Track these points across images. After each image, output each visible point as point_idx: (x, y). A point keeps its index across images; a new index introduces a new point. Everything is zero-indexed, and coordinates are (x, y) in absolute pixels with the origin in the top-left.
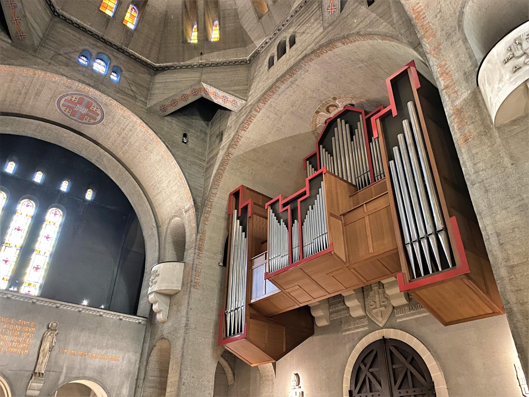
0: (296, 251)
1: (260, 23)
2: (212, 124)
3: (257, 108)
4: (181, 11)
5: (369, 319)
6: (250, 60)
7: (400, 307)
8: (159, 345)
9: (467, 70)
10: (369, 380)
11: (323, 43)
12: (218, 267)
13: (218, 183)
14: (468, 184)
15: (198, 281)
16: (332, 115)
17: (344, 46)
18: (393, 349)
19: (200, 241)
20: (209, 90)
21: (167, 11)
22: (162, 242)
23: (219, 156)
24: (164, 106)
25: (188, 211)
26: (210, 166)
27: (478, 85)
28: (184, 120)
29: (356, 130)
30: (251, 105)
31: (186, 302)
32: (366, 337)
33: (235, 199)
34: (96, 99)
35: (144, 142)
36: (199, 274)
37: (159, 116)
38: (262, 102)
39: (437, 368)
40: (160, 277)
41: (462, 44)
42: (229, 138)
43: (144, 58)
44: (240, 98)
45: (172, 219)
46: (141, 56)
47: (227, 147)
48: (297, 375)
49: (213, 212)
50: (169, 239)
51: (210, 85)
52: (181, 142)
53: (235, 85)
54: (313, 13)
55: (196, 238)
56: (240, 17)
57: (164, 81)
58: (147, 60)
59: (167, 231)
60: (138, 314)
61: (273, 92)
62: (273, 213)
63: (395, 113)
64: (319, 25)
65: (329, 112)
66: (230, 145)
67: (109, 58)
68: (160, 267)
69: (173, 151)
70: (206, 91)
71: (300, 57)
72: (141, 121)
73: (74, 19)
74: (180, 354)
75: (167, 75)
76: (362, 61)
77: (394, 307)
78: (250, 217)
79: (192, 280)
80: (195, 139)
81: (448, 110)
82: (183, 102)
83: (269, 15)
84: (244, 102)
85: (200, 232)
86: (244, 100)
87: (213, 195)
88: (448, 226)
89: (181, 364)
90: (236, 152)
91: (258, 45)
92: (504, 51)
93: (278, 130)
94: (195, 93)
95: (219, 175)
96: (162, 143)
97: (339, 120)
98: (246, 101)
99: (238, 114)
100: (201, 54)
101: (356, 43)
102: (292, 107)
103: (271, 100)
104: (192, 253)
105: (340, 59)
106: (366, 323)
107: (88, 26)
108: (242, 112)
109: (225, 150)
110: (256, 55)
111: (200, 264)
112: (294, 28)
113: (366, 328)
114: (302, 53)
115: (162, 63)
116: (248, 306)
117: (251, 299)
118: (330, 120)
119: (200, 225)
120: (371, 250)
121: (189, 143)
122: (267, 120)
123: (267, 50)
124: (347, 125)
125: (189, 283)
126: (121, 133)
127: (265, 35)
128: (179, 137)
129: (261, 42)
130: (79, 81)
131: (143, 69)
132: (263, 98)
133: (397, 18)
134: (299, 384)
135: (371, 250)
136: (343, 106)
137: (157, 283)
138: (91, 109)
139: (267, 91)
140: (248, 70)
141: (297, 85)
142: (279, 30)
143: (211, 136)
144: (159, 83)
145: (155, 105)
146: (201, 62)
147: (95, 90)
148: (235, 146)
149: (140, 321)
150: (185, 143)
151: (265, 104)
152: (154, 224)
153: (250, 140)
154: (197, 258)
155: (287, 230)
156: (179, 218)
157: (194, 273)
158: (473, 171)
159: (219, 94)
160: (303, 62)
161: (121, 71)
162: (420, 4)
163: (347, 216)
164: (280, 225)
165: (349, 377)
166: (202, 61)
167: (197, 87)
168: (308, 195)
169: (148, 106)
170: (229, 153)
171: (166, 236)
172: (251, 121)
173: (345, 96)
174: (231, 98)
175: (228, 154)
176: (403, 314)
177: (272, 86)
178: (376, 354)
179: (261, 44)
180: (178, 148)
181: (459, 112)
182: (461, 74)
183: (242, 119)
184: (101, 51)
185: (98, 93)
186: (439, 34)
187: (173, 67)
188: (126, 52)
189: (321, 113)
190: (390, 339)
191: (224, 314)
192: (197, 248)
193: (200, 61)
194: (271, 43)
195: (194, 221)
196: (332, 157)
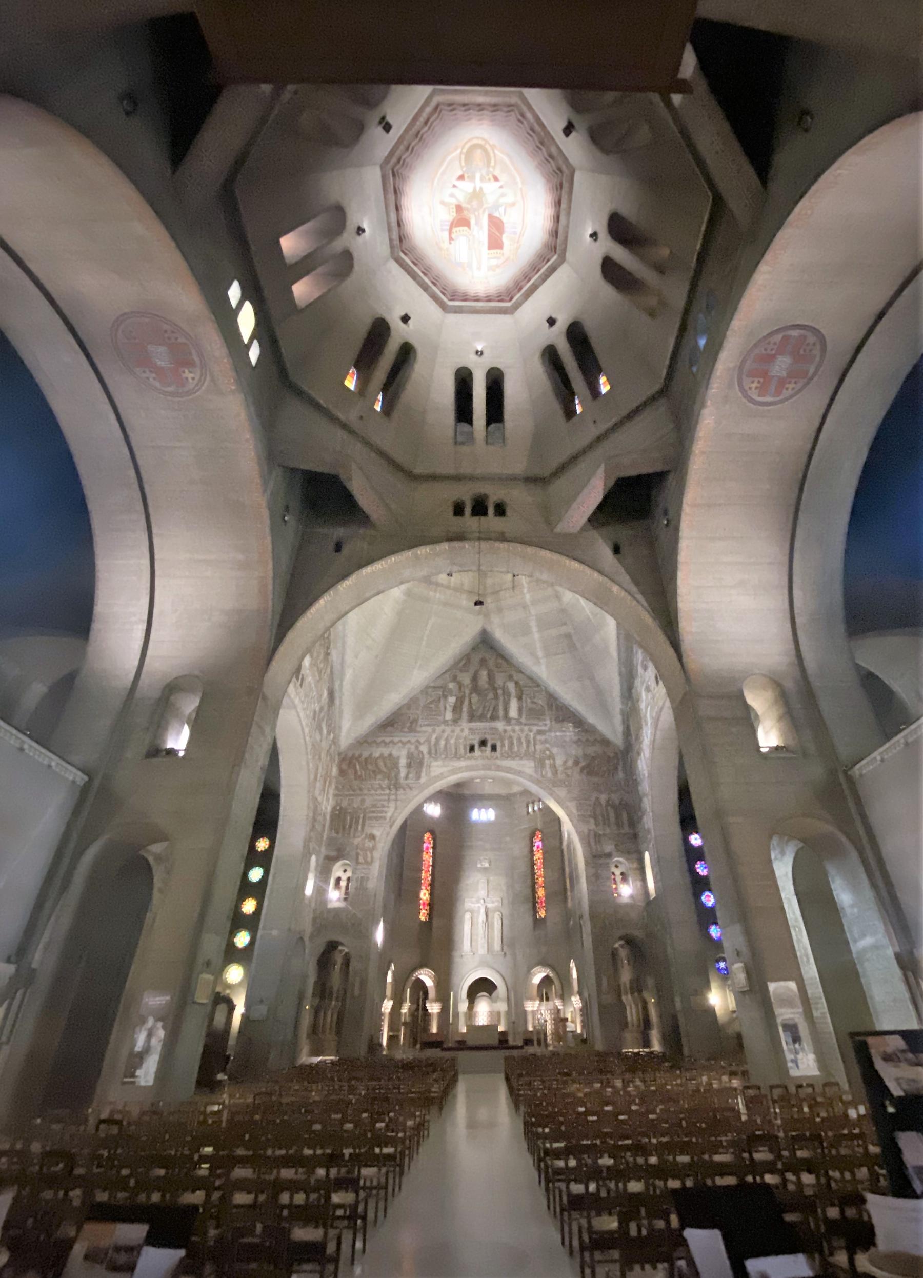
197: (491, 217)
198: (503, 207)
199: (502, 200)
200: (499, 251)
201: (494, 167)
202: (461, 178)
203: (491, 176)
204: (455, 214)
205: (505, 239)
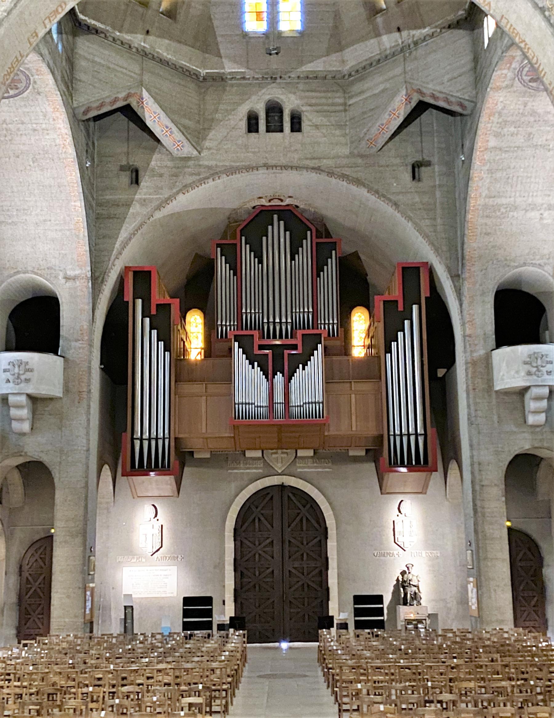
2: (100, 129)
6: (205, 79)
11: (347, 173)
12: (98, 370)
18: (290, 495)
20: (147, 104)
23: (131, 210)
26: (109, 218)
30: (209, 168)
39: (333, 517)
40: (35, 373)
44: (192, 145)
48: (153, 505)
51: (155, 99)
53: (185, 116)
54: (333, 108)
57: (91, 57)
70: (143, 103)
71: (311, 163)
84: (195, 153)
86: (197, 150)
90: (158, 215)
92: (526, 355)
97: (275, 217)
98: (200, 153)
106: (262, 465)
108: (188, 167)
113: (261, 471)
114: (314, 161)
115: (89, 18)
118: (264, 208)
124: (288, 233)
129: (234, 68)
134: (156, 516)
135: (354, 429)
140: (200, 94)
142: (271, 78)
146: (144, 47)
158: (473, 415)
159: (162, 119)
160: (309, 170)
164: (253, 368)
165: (235, 516)
166: (145, 45)
174: (178, 135)
179: (234, 71)
182: (482, 333)
183: (189, 180)
186: (478, 286)
187: (102, 32)
193: (142, 44)
194: (250, 84)
195: (86, 301)
196: (260, 265)
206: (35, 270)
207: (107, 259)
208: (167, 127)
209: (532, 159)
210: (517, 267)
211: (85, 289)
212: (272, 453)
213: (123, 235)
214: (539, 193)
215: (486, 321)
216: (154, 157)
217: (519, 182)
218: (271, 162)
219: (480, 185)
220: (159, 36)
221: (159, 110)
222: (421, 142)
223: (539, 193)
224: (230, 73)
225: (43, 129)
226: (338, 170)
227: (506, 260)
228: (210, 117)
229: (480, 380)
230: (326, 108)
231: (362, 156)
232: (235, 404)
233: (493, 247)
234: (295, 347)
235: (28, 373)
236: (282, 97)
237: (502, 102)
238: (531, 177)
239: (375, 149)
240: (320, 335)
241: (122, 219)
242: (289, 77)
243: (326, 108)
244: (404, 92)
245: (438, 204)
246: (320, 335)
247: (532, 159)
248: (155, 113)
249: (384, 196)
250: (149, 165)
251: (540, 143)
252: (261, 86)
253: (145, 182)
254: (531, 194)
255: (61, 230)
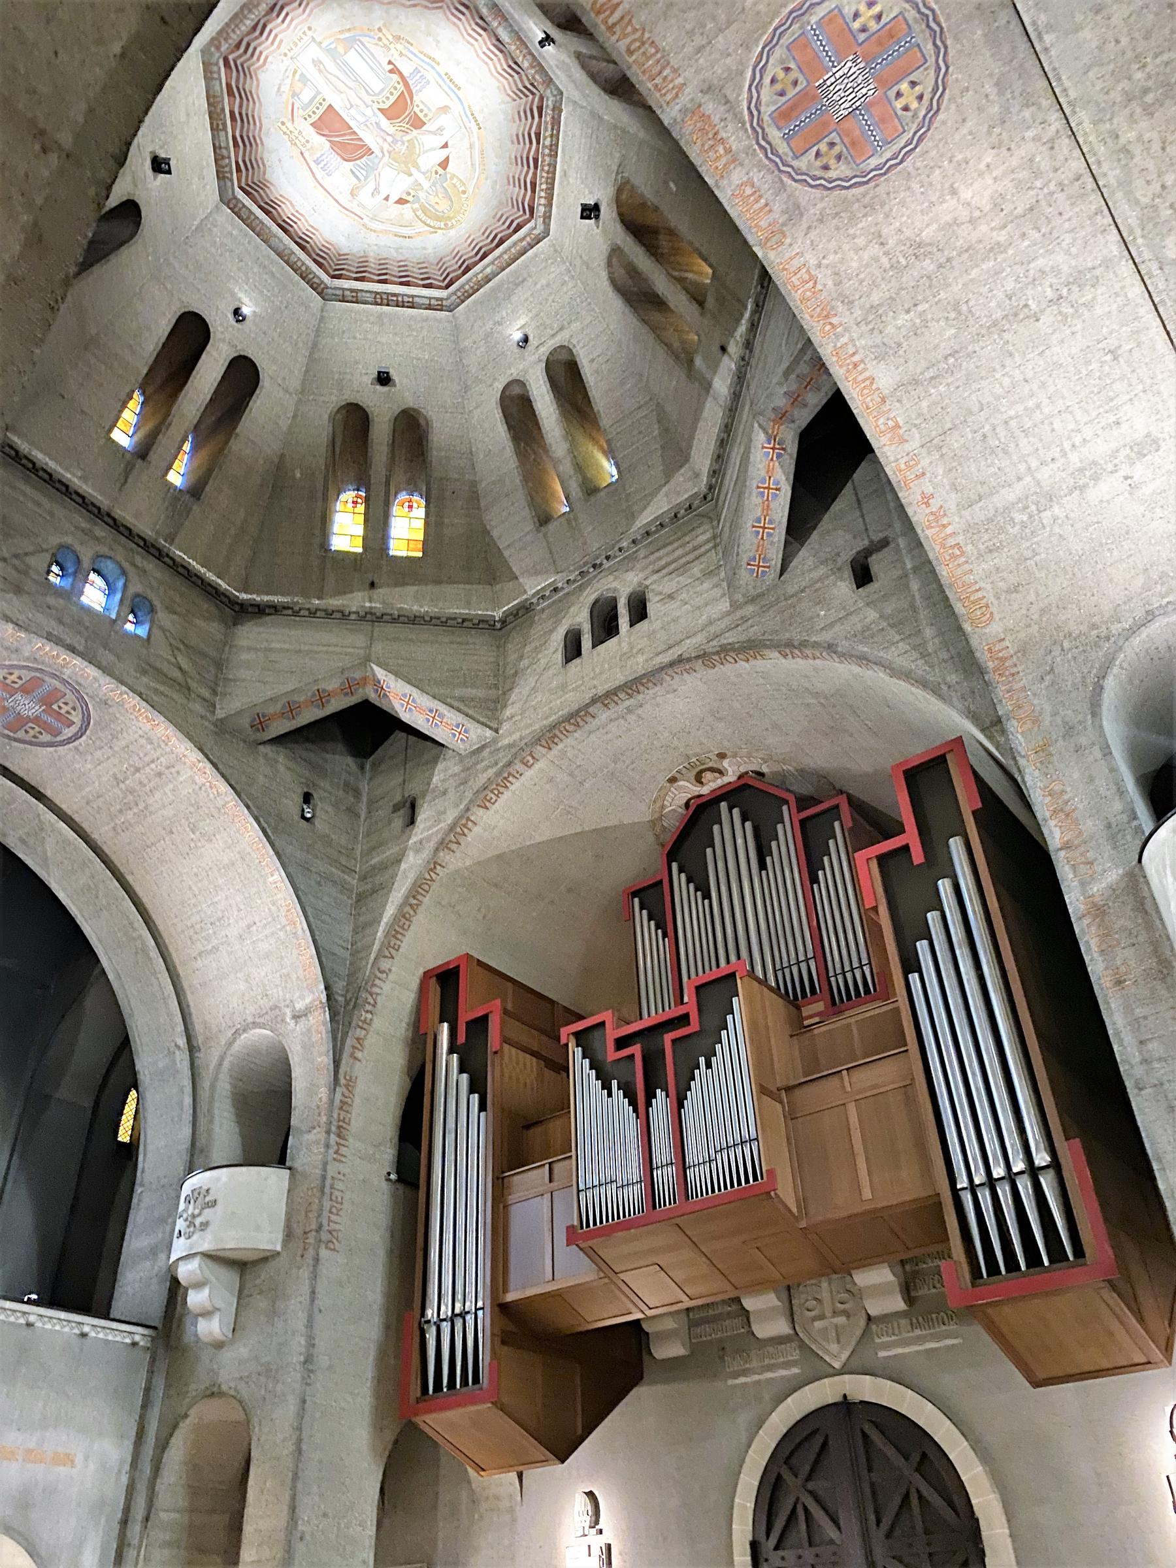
0: (665, 1176)
1: (541, 535)
2: (374, 765)
3: (529, 758)
4: (322, 462)
5: (803, 1346)
6: (503, 622)
7: (885, 1318)
8: (202, 1413)
9: (1113, 820)
10: (806, 1509)
11: (730, 641)
12: (385, 1185)
13: (398, 943)
14: (1129, 1084)
15: (337, 1227)
16: (705, 790)
17: (784, 660)
18: (867, 1428)
19: (341, 1108)
21: (282, 456)
22: (204, 1094)
23: (403, 866)
24: (264, 716)
25: (306, 1015)
26: (374, 891)
27: (1140, 861)
28: (305, 754)
29: (774, 844)
30: (510, 746)
31: (306, 1289)
32: (795, 1395)
33: (438, 989)
34: (79, 684)
35: (192, 809)
36: (338, 1206)
37: (245, 741)
38: (544, 743)
40: (219, 1208)
41: (1100, 756)
42: (440, 821)
43: (211, 576)
44: (478, 722)
45: (244, 1031)
46: (203, 570)
47: (432, 845)
48: (591, 1495)
49: (377, 1023)
50: (224, 1087)
51: (397, 674)
52: (297, 817)
53: (464, 685)
54: (697, 553)
55: (331, 1101)
56: (482, 504)
58: (219, 581)
59: (220, 1064)
60: (112, 1316)
61: (578, 725)
62: (584, 1057)
63: (918, 856)
64: (717, 592)
65: (701, 783)
66: (442, 842)
67: (124, 573)
68: (218, 1179)
69: (277, 844)
71: (666, 658)
72: (201, 756)
73: (39, 456)
74: (290, 1446)
75: (273, 630)
76: (816, 695)
77: (869, 1318)
78: (496, 1053)
79: (320, 1226)
80: (330, 809)
81: (1074, 900)
82: (316, 710)
83: (569, 521)
84: (489, 733)
85: (343, 1081)
86: (490, 728)
87: (379, 975)
88: (1062, 1161)
89: (296, 1477)
90: (454, 861)
91: (531, 588)
93: (569, 812)
94: (349, 687)
95: (403, 920)
96: (251, 820)
97: (724, 805)
98: (497, 731)
99: (468, 762)
100: (372, 585)
101: (818, 661)
102: (616, 763)
103: (569, 741)
104: (317, 1142)
105: (762, 681)
106: (796, 1355)
107: (75, 480)
109: (426, 854)
110: (524, 611)
111: (340, 1177)
112: (641, 575)
113: (796, 1370)
114: (671, 651)
116: (497, 1309)
117: (505, 1291)
118: (700, 801)
119: (343, 1062)
120: (867, 1194)
121: (317, 822)
122: (547, 787)
123: (558, 611)
124: (748, 825)
125: (314, 1233)
126: (126, 778)
127: (552, 568)
128: (292, 803)
130: (49, 637)
131: (206, 606)
132: (549, 736)
133: (936, 641)
134: (597, 1522)
135: (867, 1194)
136: (738, 774)
137: (209, 1229)
138: (55, 707)
139: (563, 722)
140: (498, 647)
141: (639, 716)
142: (594, 566)
143: (371, 803)
144: (249, 649)
145: (239, 713)
146: (371, 608)
147: (86, 663)
148: (454, 846)
149: (137, 1338)
150: (307, 820)
151: (550, 749)
152: (182, 1041)
153: (495, 832)
154: (335, 1159)
155: (633, 1115)
156: (269, 1032)
157: (327, 1204)
159: (418, 701)
160: (670, 671)
161: (152, 610)
162: (1007, 643)
163: (798, 1093)
164: (610, 1095)
167: (357, 675)
168: (694, 1026)
169: (220, 714)
170: (435, 863)
171: (216, 1079)
172: (506, 787)
173: (749, 753)
175: (433, 865)
176: (894, 1338)
177: (578, 711)
178: (825, 1445)
180: (290, 835)
181: (1099, 911)
182: (1101, 825)
183: (482, 779)
184: (104, 550)
185: (92, 671)
187: (288, 608)
188: (168, 555)
189: (681, 783)
190: (862, 1402)
191: (416, 1325)
192: (334, 1129)
193: (368, 604)
195: (324, 1049)
196: (706, 901)
197: (370, 152)
198: (362, 178)
199: (371, 186)
200: (315, 118)
201: (414, 211)
202: (444, 164)
203: (410, 198)
204: (416, 110)
205: (320, 142)
206: (257, 1020)
207: (364, 963)
208: (431, 711)
209: (1008, 362)
210: (1134, 630)
211: (322, 1028)
212: (814, 1319)
213: (390, 911)
214: (1088, 432)
215: (1102, 791)
216: (436, 772)
217: (1017, 433)
218: (601, 690)
219: (929, 489)
220: (396, 585)
221: (408, 689)
222: (862, 516)
223: (1088, 432)
224: (534, 595)
225: (168, 768)
226: (715, 643)
227: (1094, 626)
228: (512, 672)
229: (1129, 953)
230: (684, 560)
231: (752, 600)
232: (579, 1191)
233: (1043, 611)
234: (684, 1019)
235: (207, 1211)
236: (615, 584)
237: (819, 266)
238: (1038, 406)
239: (773, 574)
240: (733, 975)
241: (383, 889)
242: (620, 550)
243: (684, 560)
244: (762, 437)
245: (918, 602)
246: (733, 975)
247: (1008, 362)
248: (405, 695)
249: (803, 644)
250: (429, 784)
251: (999, 314)
252: (581, 588)
253: (424, 815)
254: (1067, 446)
255: (273, 934)
